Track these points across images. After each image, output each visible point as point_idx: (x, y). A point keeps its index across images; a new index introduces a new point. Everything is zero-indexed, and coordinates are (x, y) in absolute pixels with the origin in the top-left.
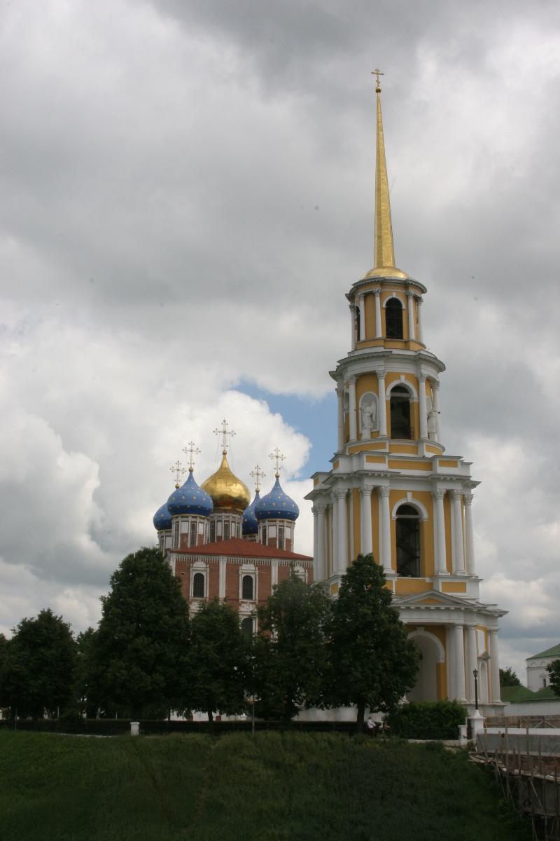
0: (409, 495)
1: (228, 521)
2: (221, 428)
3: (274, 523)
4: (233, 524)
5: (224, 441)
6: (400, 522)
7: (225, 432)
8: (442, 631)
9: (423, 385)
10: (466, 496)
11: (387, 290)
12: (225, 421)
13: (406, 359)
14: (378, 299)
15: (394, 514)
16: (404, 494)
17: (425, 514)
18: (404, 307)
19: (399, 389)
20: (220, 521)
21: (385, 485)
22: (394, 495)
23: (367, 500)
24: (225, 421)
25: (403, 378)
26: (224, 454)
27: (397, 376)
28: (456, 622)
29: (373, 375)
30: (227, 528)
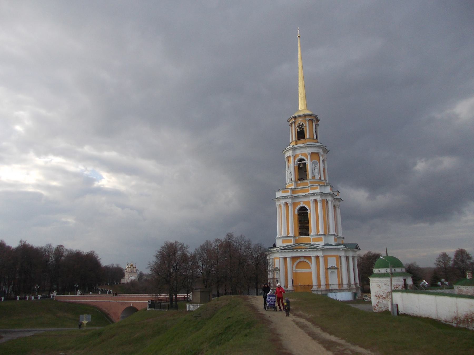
0: (302, 203)
6: (299, 214)
8: (309, 258)
9: (309, 157)
10: (327, 200)
13: (289, 150)
14: (293, 125)
15: (296, 212)
16: (299, 203)
21: (289, 201)
22: (294, 204)
25: (300, 155)
27: (298, 155)
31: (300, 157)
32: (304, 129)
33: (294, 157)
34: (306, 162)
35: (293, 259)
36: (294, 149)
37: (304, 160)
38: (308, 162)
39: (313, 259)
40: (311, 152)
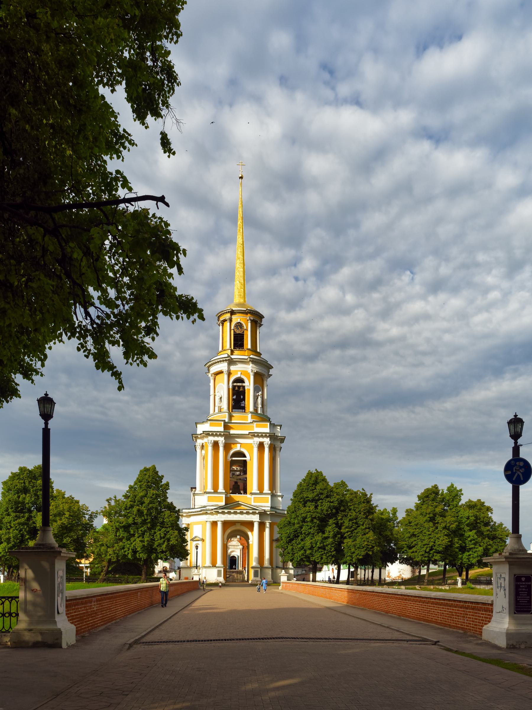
8: (250, 524)
11: (234, 317)
17: (248, 458)
18: (245, 328)
19: (240, 380)
22: (227, 447)
23: (210, 449)
28: (254, 520)
29: (221, 372)
31: (238, 375)
32: (243, 332)
33: (229, 374)
34: (246, 384)
35: (226, 524)
36: (231, 362)
37: (242, 381)
38: (249, 385)
39: (256, 526)
40: (255, 371)
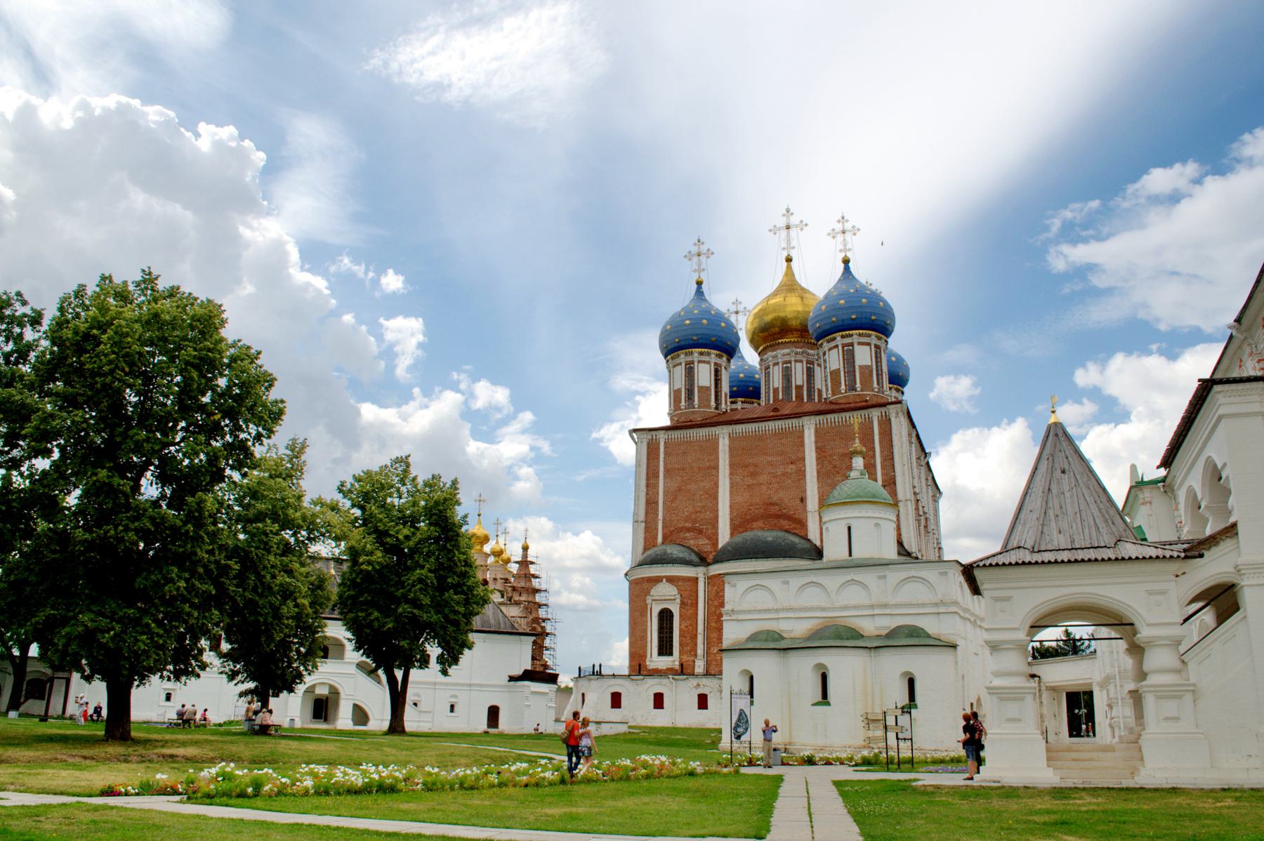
1: (790, 362)
2: (782, 222)
3: (833, 344)
4: (799, 365)
5: (789, 240)
7: (788, 228)
12: (788, 211)
20: (778, 364)
24: (788, 211)
26: (789, 260)
30: (787, 376)
